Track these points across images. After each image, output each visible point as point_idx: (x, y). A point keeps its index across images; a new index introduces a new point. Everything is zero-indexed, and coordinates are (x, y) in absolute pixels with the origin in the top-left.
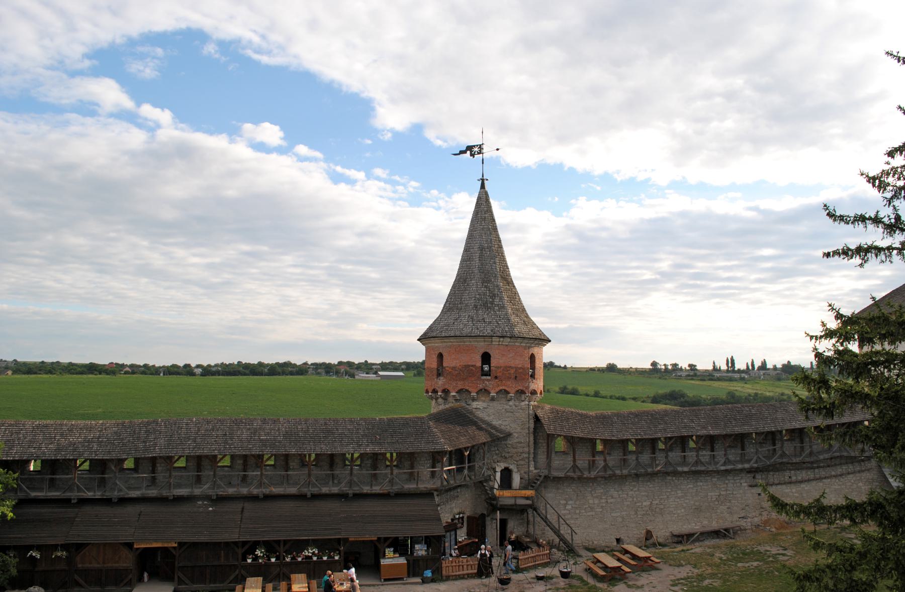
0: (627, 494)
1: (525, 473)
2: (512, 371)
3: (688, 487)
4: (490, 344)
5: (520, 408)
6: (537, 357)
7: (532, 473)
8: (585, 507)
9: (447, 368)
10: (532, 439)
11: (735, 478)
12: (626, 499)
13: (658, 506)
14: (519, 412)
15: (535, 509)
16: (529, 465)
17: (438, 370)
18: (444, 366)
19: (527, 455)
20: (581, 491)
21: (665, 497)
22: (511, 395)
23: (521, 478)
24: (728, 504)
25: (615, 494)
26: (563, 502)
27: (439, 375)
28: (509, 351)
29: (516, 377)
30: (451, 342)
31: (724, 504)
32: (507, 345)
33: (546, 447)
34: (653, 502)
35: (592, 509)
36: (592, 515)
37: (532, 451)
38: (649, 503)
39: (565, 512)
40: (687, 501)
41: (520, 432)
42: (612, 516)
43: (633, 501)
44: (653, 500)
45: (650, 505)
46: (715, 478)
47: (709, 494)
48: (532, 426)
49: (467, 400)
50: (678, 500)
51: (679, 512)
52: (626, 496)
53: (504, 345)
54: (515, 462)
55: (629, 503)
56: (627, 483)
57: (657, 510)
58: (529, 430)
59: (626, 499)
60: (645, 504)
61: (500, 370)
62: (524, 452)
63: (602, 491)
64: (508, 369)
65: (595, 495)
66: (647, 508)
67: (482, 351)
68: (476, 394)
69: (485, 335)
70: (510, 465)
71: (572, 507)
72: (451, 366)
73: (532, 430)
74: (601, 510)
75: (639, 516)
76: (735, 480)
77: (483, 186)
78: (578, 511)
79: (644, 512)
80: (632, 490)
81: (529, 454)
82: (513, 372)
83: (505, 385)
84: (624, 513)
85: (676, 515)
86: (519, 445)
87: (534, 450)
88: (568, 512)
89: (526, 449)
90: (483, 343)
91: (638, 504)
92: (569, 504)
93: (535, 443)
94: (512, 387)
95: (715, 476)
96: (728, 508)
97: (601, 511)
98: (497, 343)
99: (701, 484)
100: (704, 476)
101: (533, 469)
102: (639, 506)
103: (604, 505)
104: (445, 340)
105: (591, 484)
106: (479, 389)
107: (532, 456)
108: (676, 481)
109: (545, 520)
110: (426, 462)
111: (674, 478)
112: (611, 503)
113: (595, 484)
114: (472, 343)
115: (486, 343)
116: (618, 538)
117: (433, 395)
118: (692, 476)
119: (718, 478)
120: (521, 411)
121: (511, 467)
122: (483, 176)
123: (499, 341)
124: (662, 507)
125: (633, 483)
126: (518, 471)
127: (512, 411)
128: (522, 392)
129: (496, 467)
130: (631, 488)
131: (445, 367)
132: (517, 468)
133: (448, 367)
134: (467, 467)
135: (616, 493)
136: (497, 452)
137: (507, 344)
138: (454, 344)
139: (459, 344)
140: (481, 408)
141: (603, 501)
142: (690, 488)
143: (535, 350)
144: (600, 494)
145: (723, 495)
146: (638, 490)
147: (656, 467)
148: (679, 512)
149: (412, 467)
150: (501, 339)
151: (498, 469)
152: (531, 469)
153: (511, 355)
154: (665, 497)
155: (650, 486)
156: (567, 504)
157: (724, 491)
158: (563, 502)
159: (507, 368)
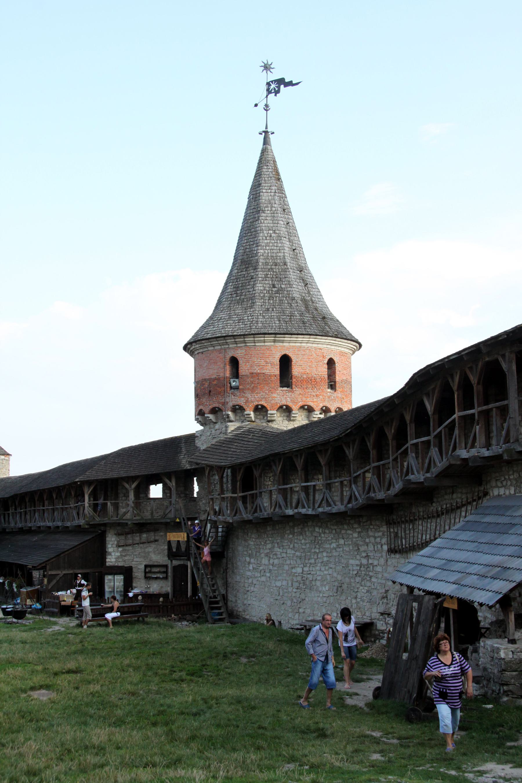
3: (332, 547)
11: (376, 535)
24: (368, 584)
29: (210, 391)
32: (202, 353)
40: (330, 571)
42: (276, 586)
43: (290, 564)
45: (302, 573)
46: (356, 532)
47: (352, 562)
50: (323, 569)
51: (324, 589)
66: (299, 578)
75: (295, 590)
76: (375, 538)
77: (266, 141)
84: (284, 583)
91: (294, 571)
95: (356, 528)
96: (368, 591)
100: (346, 527)
108: (323, 535)
118: (336, 527)
119: (359, 532)
122: (266, 128)
124: (310, 577)
143: (239, 354)
145: (364, 565)
146: (294, 546)
153: (206, 364)
154: (313, 561)
158: (248, 559)
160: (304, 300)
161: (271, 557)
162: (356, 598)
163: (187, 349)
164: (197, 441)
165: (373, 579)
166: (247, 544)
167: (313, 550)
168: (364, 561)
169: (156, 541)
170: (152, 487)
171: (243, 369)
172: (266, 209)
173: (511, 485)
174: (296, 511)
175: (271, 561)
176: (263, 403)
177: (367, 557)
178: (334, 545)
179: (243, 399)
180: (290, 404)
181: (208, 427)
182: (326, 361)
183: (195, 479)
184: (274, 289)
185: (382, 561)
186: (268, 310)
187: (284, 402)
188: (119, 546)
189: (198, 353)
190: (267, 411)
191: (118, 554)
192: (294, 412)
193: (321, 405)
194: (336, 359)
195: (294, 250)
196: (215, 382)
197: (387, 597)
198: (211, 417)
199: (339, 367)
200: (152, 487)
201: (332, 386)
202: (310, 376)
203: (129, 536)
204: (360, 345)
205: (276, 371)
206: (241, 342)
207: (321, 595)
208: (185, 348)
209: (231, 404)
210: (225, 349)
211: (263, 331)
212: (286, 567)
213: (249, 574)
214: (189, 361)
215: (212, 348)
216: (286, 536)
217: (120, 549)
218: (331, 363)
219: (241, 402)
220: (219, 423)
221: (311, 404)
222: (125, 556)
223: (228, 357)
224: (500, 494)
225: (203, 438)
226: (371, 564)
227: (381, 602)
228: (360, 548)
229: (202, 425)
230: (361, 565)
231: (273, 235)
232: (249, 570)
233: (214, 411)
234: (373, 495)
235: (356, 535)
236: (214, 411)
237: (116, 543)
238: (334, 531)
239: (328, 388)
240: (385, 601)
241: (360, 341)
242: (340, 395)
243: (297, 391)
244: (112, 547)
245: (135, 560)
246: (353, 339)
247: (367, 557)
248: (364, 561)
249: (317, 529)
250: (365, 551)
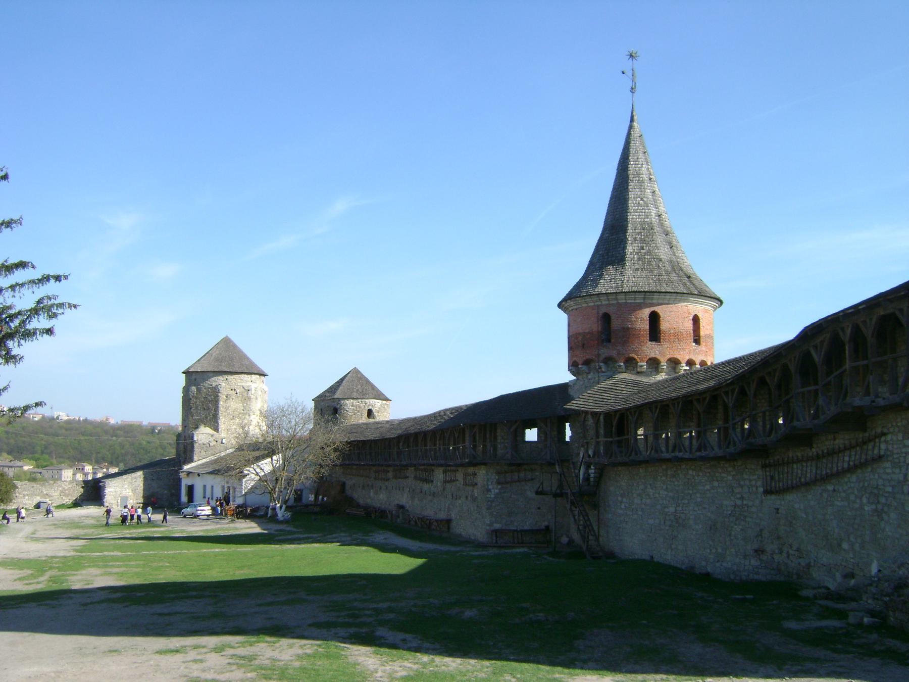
2: (580, 338)
3: (706, 488)
11: (752, 477)
21: (686, 501)
24: (743, 523)
31: (737, 522)
32: (576, 309)
47: (725, 502)
51: (697, 527)
66: (672, 517)
75: (667, 528)
76: (750, 481)
91: (666, 510)
96: (742, 530)
108: (696, 478)
118: (709, 470)
137: (575, 307)
142: (707, 490)
146: (667, 488)
148: (697, 527)
153: (579, 320)
154: (686, 501)
157: (739, 499)
158: (620, 499)
160: (671, 261)
161: (644, 496)
162: (730, 535)
163: (561, 305)
164: (570, 390)
165: (748, 519)
166: (619, 485)
167: (686, 492)
168: (739, 502)
169: (532, 479)
170: (527, 431)
171: (615, 324)
172: (634, 179)
173: (899, 431)
174: (673, 454)
175: (644, 500)
176: (633, 355)
177: (742, 498)
178: (708, 487)
179: (615, 352)
180: (659, 357)
181: (580, 377)
182: (691, 318)
183: (567, 425)
184: (642, 251)
185: (757, 502)
186: (637, 270)
187: (653, 355)
188: (499, 483)
189: (572, 310)
190: (638, 362)
191: (497, 491)
192: (662, 364)
193: (687, 358)
194: (700, 316)
195: (659, 216)
197: (761, 535)
198: (584, 368)
199: (702, 323)
200: (527, 431)
201: (697, 341)
202: (677, 331)
203: (507, 475)
204: (721, 302)
205: (645, 326)
206: (613, 299)
207: (694, 533)
208: (560, 305)
209: (603, 356)
210: (598, 306)
211: (635, 289)
212: (659, 507)
213: (620, 512)
214: (563, 317)
215: (586, 305)
216: (659, 477)
217: (499, 487)
218: (696, 320)
219: (614, 353)
220: (592, 374)
221: (679, 357)
222: (504, 492)
223: (601, 313)
224: (887, 440)
225: (577, 387)
226: (746, 505)
227: (755, 540)
228: (735, 490)
229: (575, 376)
230: (735, 506)
231: (641, 202)
232: (621, 509)
233: (587, 362)
234: (753, 440)
235: (730, 478)
236: (587, 362)
237: (495, 480)
238: (708, 474)
239: (694, 342)
240: (760, 538)
241: (721, 299)
242: (704, 349)
243: (665, 345)
244: (492, 484)
245: (512, 496)
246: (716, 297)
247: (742, 498)
248: (739, 502)
249: (690, 472)
250: (739, 493)
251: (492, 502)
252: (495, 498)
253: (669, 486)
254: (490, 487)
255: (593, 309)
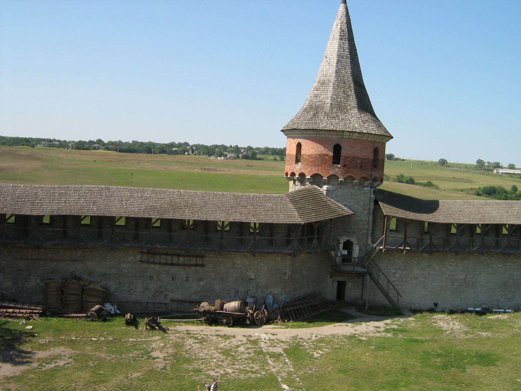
0: (447, 269)
1: (364, 245)
2: (359, 161)
4: (341, 138)
5: (363, 192)
6: (380, 151)
7: (369, 246)
8: (411, 276)
9: (304, 156)
10: (371, 218)
12: (445, 272)
13: (471, 279)
14: (361, 195)
15: (370, 275)
16: (367, 239)
17: (297, 157)
18: (302, 153)
19: (365, 231)
20: (408, 264)
22: (356, 181)
23: (360, 250)
25: (437, 267)
26: (393, 271)
27: (297, 161)
28: (357, 144)
29: (361, 166)
30: (309, 134)
32: (355, 139)
33: (382, 226)
34: (467, 276)
35: (416, 278)
36: (416, 283)
37: (371, 228)
38: (464, 277)
39: (394, 279)
41: (362, 212)
44: (467, 275)
48: (372, 207)
49: (320, 183)
52: (445, 269)
53: (353, 139)
54: (356, 236)
55: (447, 276)
56: (447, 260)
57: (470, 283)
58: (369, 211)
59: (445, 272)
60: (460, 277)
61: (348, 160)
62: (364, 229)
63: (426, 264)
64: (355, 159)
65: (420, 267)
67: (335, 143)
68: (327, 179)
69: (337, 129)
70: (352, 239)
71: (400, 275)
72: (308, 154)
73: (371, 211)
74: (424, 279)
75: (455, 287)
78: (404, 279)
79: (460, 284)
80: (451, 265)
81: (368, 230)
82: (359, 162)
83: (351, 173)
85: (486, 288)
86: (360, 223)
87: (373, 227)
88: (396, 279)
89: (366, 227)
90: (335, 137)
91: (455, 277)
92: (398, 273)
93: (374, 222)
94: (357, 174)
97: (424, 281)
98: (348, 137)
99: (509, 264)
100: (512, 257)
101: (371, 242)
102: (456, 278)
103: (427, 276)
104: (304, 132)
105: (417, 258)
106: (330, 174)
107: (370, 232)
108: (489, 260)
109: (377, 283)
110: (283, 232)
111: (487, 258)
112: (433, 275)
113: (421, 259)
114: (326, 136)
115: (338, 136)
116: (436, 302)
117: (292, 177)
120: (363, 195)
121: (354, 240)
123: (349, 136)
124: (474, 280)
125: (452, 260)
126: (358, 244)
127: (356, 194)
128: (365, 179)
129: (340, 239)
130: (450, 263)
131: (302, 155)
132: (357, 241)
133: (305, 155)
134: (316, 238)
135: (437, 266)
136: (342, 227)
137: (356, 138)
138: (311, 136)
139: (315, 136)
140: (331, 190)
141: (427, 272)
144: (424, 267)
147: (472, 248)
149: (271, 235)
150: (351, 134)
151: (342, 241)
152: (368, 242)
155: (466, 263)
156: (396, 273)
158: (393, 271)
159: (354, 158)
191: (290, 273)
196: (366, 161)
222: (293, 274)
223: (375, 146)
251: (286, 282)
252: (288, 279)
253: (458, 265)
254: (287, 271)
255: (371, 143)
